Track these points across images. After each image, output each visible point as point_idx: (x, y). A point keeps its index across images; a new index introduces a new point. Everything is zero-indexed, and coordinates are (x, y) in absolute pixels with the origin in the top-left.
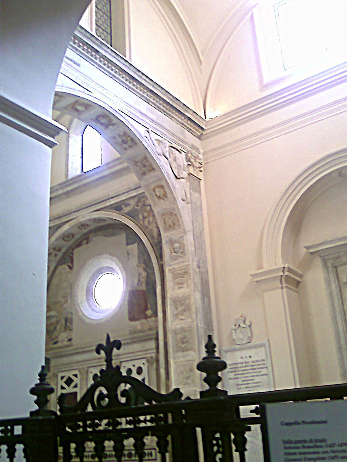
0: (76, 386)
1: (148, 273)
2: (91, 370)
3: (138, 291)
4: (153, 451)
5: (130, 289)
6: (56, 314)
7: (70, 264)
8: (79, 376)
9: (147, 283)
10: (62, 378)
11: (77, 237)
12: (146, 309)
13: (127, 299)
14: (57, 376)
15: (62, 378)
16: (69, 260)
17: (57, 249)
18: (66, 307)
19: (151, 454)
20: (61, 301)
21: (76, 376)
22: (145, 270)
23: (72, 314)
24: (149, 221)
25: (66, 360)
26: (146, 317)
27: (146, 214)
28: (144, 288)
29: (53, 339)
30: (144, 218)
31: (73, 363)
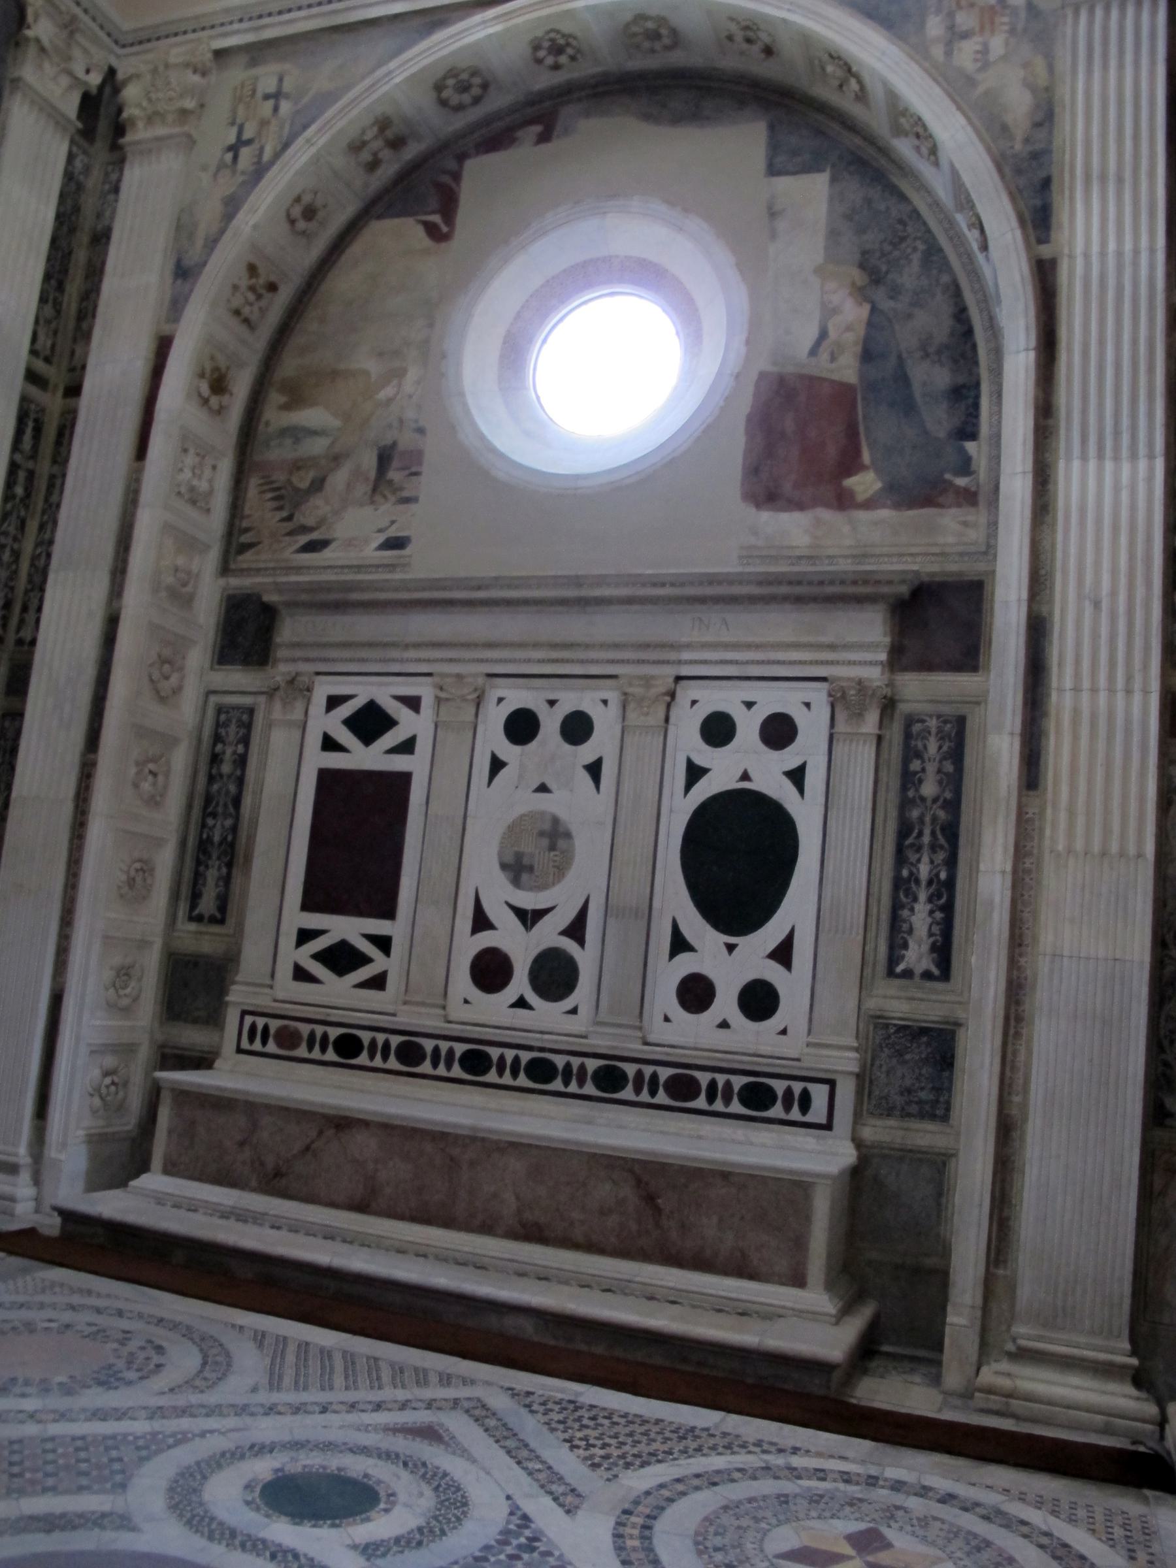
0: (407, 747)
1: (874, 310)
2: (502, 689)
3: (812, 381)
4: (819, 1094)
5: (763, 364)
6: (337, 423)
7: (436, 218)
8: (427, 704)
9: (868, 355)
10: (333, 702)
11: (495, 102)
12: (850, 463)
13: (745, 404)
14: (309, 690)
15: (333, 702)
16: (434, 202)
17: (389, 134)
18: (390, 401)
19: (805, 1102)
20: (366, 373)
21: (413, 703)
22: (861, 293)
23: (421, 431)
24: (985, 50)
25: (365, 626)
26: (843, 501)
27: (965, 20)
28: (847, 370)
29: (304, 529)
30: (955, 36)
31: (407, 646)
